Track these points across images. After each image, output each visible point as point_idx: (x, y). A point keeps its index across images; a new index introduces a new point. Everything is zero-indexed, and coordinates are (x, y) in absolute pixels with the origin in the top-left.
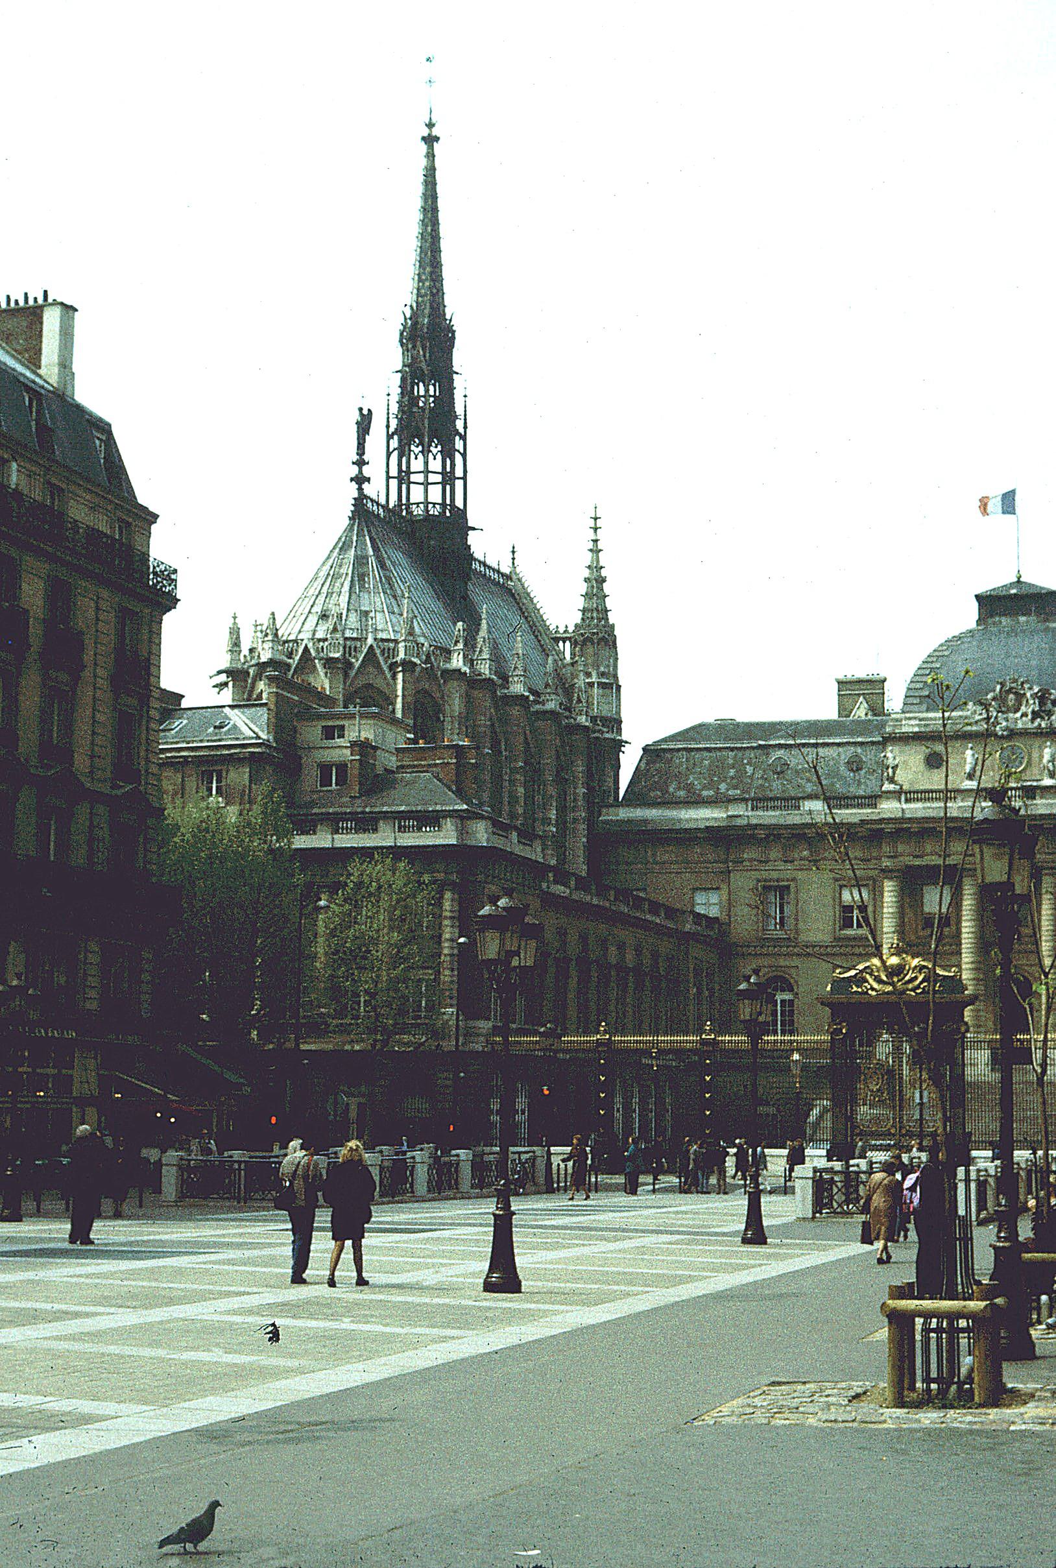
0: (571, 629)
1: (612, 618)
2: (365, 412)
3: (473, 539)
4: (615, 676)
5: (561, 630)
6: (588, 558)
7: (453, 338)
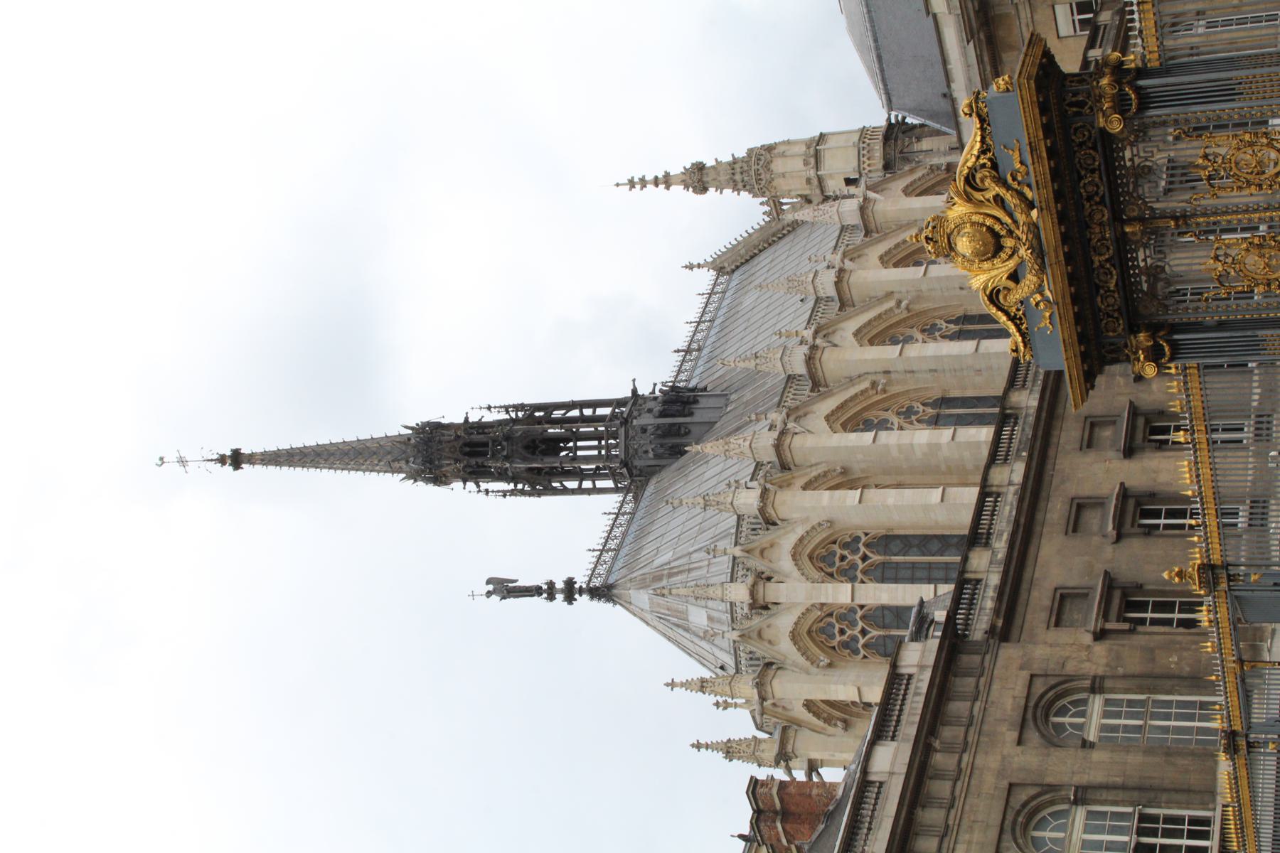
0: (764, 199)
1: (741, 153)
2: (491, 587)
3: (644, 390)
4: (808, 143)
5: (767, 208)
6: (677, 189)
7: (428, 424)
